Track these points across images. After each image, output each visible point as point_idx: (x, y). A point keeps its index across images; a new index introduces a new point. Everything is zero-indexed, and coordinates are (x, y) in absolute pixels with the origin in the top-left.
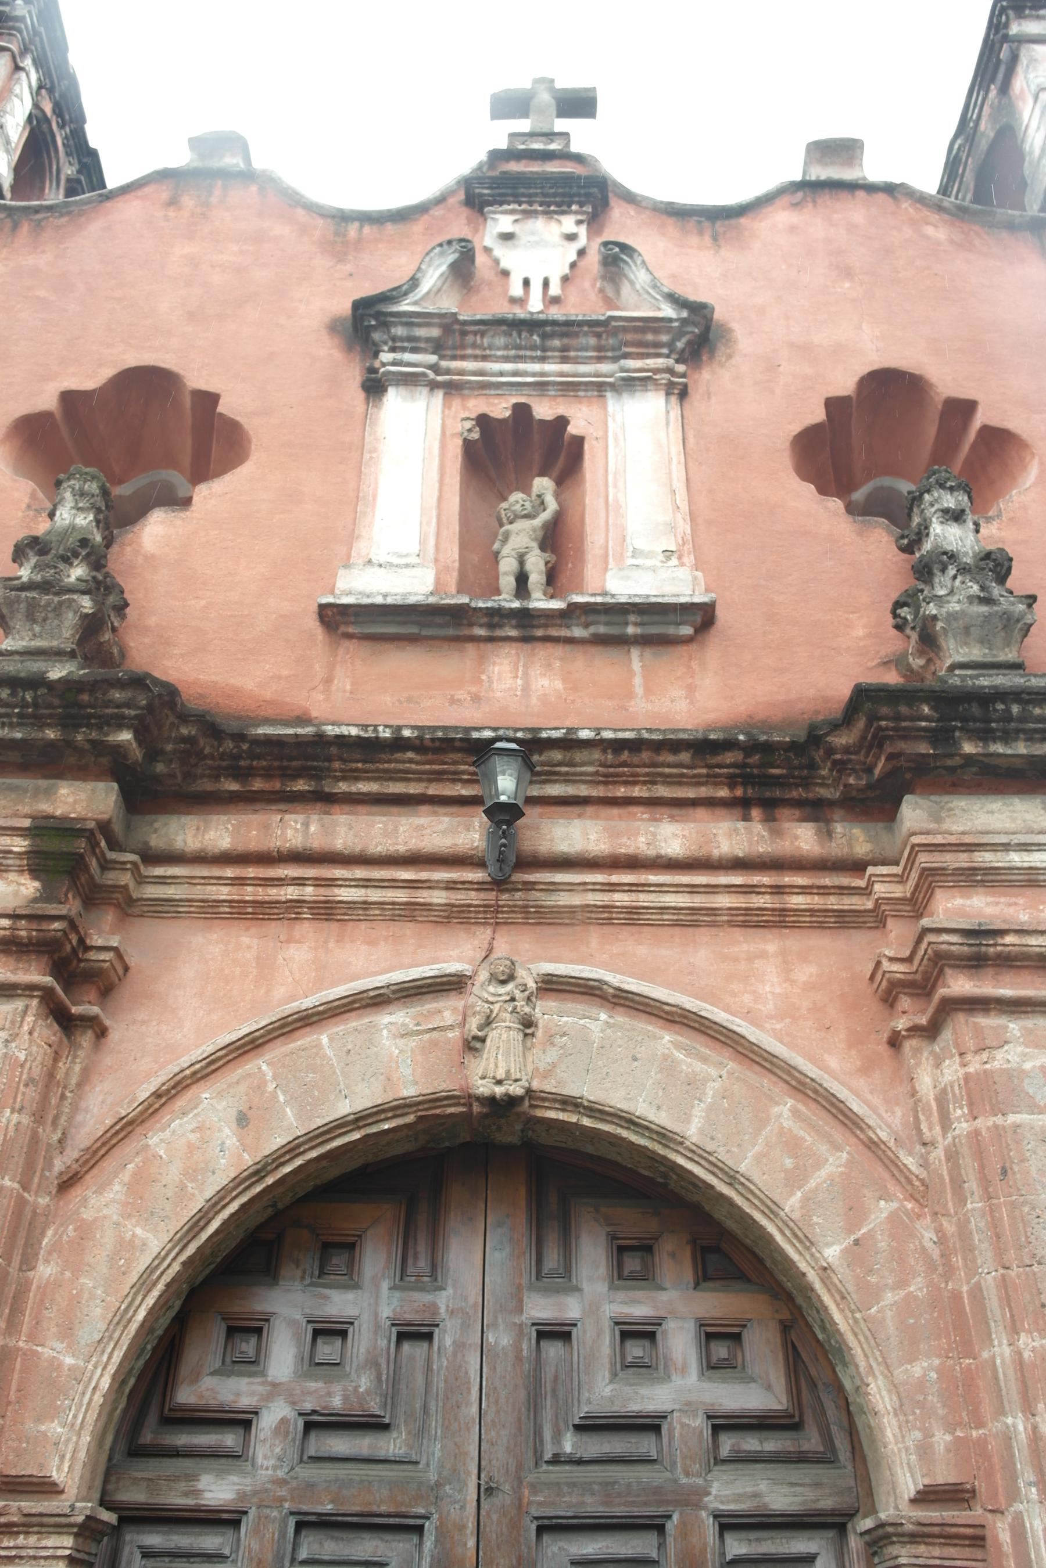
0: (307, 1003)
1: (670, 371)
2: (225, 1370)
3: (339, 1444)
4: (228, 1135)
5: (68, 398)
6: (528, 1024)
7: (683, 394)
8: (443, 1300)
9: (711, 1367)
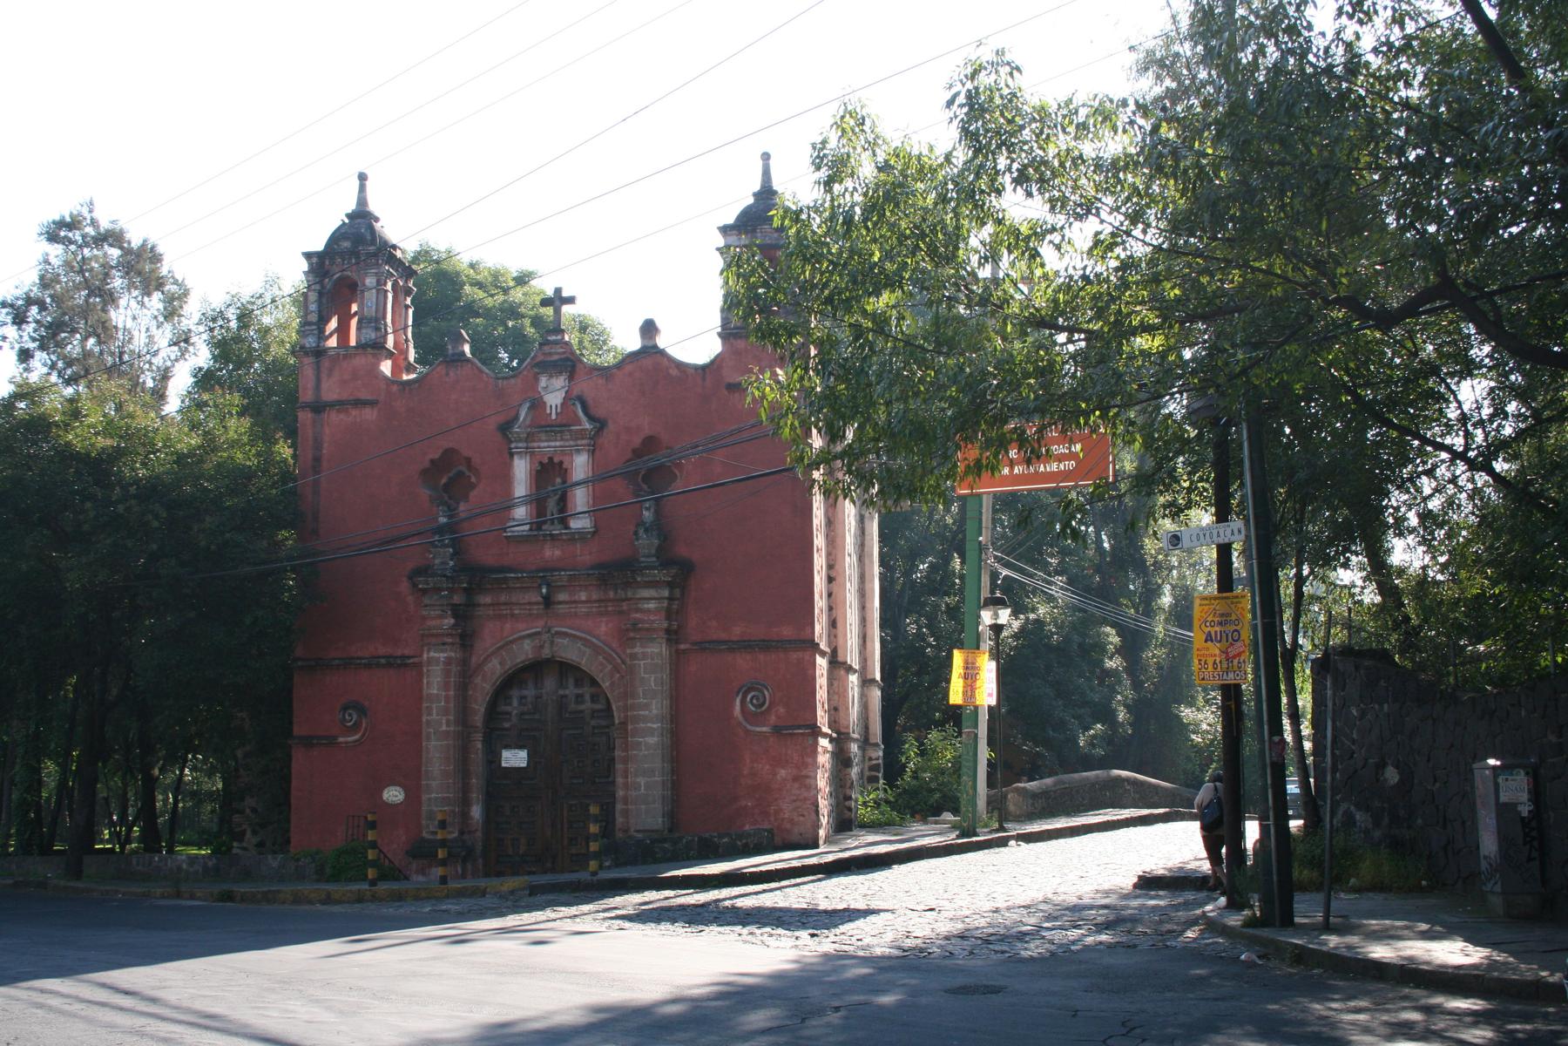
0: (511, 638)
1: (589, 445)
2: (506, 705)
3: (527, 717)
4: (498, 667)
5: (432, 461)
6: (552, 643)
7: (594, 450)
8: (544, 691)
9: (593, 701)
